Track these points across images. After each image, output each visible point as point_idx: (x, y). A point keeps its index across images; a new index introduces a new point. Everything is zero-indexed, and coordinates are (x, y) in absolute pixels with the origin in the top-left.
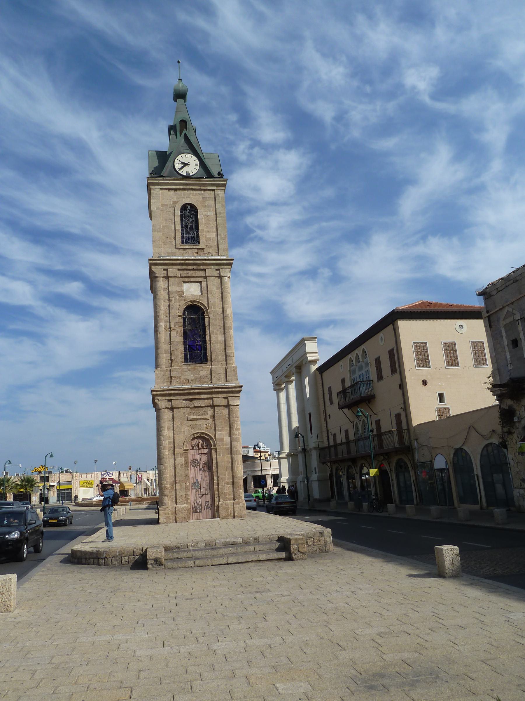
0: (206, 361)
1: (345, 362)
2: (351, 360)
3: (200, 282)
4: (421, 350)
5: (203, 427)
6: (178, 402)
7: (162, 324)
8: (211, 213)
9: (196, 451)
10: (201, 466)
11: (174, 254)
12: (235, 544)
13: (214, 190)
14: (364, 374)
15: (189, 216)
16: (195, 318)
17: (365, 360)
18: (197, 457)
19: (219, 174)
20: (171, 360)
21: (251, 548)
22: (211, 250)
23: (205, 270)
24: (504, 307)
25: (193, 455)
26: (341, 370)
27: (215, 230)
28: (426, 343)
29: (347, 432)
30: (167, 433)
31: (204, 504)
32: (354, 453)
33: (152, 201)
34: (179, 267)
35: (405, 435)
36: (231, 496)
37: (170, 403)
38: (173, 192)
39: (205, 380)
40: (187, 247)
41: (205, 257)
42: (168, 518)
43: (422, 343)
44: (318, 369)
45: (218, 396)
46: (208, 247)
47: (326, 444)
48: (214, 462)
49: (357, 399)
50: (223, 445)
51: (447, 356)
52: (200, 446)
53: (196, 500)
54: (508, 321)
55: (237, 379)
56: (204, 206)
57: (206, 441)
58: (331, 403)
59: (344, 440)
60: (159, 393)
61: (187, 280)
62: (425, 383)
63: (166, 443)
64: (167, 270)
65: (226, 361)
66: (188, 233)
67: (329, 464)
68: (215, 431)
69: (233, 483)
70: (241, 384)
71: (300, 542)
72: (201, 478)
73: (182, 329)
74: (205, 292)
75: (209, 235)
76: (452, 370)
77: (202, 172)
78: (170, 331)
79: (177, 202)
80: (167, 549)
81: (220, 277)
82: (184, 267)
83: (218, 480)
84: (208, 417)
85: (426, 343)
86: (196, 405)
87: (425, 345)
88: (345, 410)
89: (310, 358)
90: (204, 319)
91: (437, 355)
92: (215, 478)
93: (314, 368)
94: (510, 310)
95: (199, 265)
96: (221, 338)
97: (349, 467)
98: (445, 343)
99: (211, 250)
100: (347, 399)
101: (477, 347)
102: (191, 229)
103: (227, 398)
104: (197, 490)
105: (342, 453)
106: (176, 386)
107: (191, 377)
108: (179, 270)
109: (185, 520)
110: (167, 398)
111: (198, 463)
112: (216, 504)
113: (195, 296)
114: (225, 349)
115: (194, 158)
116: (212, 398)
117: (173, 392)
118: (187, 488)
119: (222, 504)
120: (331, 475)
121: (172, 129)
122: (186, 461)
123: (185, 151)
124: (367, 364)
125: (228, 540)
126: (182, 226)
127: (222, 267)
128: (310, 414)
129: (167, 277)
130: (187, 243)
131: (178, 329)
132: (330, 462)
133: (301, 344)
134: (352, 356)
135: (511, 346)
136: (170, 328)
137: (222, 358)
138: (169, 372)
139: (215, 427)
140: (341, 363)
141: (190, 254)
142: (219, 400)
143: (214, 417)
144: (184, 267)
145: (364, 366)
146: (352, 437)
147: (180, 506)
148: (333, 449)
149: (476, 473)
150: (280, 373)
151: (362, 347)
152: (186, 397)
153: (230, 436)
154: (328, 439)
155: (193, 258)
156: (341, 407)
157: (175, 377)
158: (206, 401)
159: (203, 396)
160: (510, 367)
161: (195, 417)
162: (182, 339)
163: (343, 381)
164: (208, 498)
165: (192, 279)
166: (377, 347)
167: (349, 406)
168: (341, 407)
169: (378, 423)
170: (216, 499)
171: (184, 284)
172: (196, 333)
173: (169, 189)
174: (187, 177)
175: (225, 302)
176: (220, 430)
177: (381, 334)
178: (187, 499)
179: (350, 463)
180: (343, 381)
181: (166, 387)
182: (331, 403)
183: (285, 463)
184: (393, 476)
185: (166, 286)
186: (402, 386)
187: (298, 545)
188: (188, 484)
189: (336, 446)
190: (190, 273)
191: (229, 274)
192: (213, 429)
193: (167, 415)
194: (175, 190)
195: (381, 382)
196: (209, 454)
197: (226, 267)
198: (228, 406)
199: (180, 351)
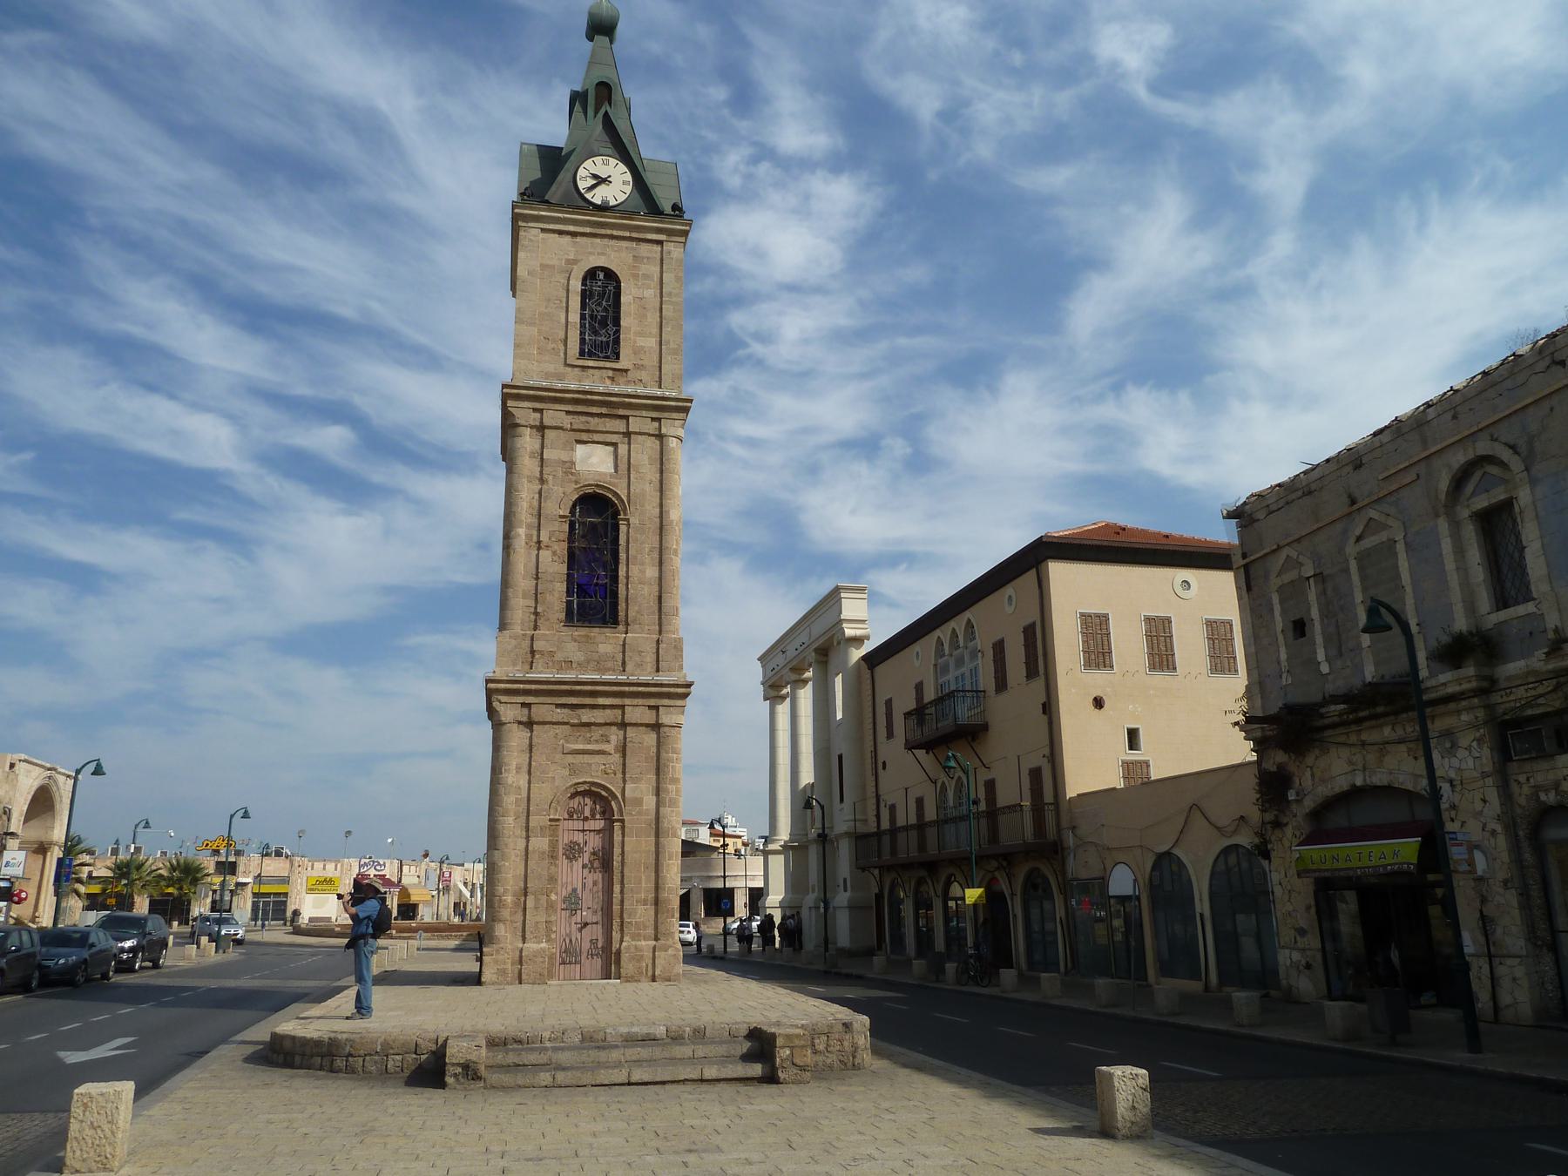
0: (616, 622)
1: (924, 648)
2: (940, 642)
3: (615, 445)
4: (1096, 630)
5: (597, 771)
7: (521, 532)
8: (651, 293)
9: (579, 825)
10: (586, 856)
11: (560, 377)
12: (649, 1040)
13: (660, 243)
14: (968, 674)
15: (601, 297)
16: (597, 523)
17: (971, 644)
18: (579, 838)
19: (675, 207)
20: (536, 614)
21: (685, 1051)
22: (644, 375)
23: (626, 418)
24: (1279, 548)
25: (570, 832)
26: (917, 664)
27: (655, 331)
28: (1106, 616)
29: (920, 802)
30: (514, 778)
31: (586, 945)
32: (932, 849)
33: (521, 255)
34: (570, 408)
35: (1050, 817)
36: (650, 931)
37: (525, 711)
38: (568, 239)
39: (609, 664)
40: (591, 363)
41: (630, 390)
42: (503, 972)
43: (1098, 616)
44: (865, 658)
45: (636, 701)
46: (638, 367)
47: (872, 827)
48: (617, 851)
49: (947, 731)
50: (640, 813)
51: (1151, 646)
52: (587, 813)
53: (569, 935)
54: (1288, 577)
55: (681, 667)
56: (636, 276)
57: (600, 802)
58: (890, 735)
59: (913, 820)
60: (502, 686)
61: (584, 437)
62: (1098, 703)
63: (510, 801)
64: (541, 411)
65: (660, 625)
66: (595, 333)
67: (876, 872)
68: (624, 781)
69: (657, 902)
70: (689, 679)
71: (797, 1042)
72: (584, 885)
73: (565, 545)
74: (625, 467)
75: (641, 342)
76: (1160, 679)
77: (638, 200)
78: (539, 549)
79: (575, 262)
80: (494, 1043)
81: (660, 436)
82: (580, 408)
83: (622, 892)
84: (609, 748)
85: (1106, 616)
86: (585, 719)
87: (1103, 619)
88: (920, 753)
89: (849, 631)
90: (616, 528)
91: (1128, 643)
92: (617, 888)
93: (856, 654)
94: (1294, 554)
95: (614, 407)
96: (651, 572)
97: (920, 882)
98: (1148, 620)
99: (644, 375)
100: (926, 729)
101: (1217, 632)
102: (603, 324)
103: (656, 708)
104: (573, 912)
105: (908, 848)
108: (568, 412)
109: (541, 980)
110: (520, 699)
111: (581, 851)
112: (615, 946)
113: (600, 474)
114: (660, 598)
115: (622, 167)
116: (622, 707)
117: (533, 687)
118: (551, 906)
119: (628, 948)
120: (879, 897)
121: (577, 99)
122: (553, 845)
123: (602, 150)
124: (974, 654)
125: (635, 1029)
126: (583, 317)
127: (666, 415)
128: (840, 757)
129: (541, 428)
130: (591, 355)
131: (556, 547)
132: (880, 868)
134: (943, 633)
135: (1290, 634)
136: (539, 542)
137: (650, 619)
138: (528, 642)
139: (624, 773)
140: (917, 647)
141: (596, 381)
142: (637, 712)
143: (623, 750)
144: (580, 408)
145: (966, 658)
146: (931, 814)
147: (531, 946)
148: (886, 839)
149: (1198, 910)
150: (780, 660)
151: (967, 615)
152: (563, 700)
153: (658, 795)
154: (878, 816)
155: (601, 389)
156: (910, 746)
157: (541, 652)
158: (608, 711)
159: (601, 701)
160: (1286, 680)
161: (581, 747)
162: (564, 568)
163: (919, 687)
164: (596, 932)
165: (596, 437)
166: (999, 618)
167: (929, 746)
168: (910, 746)
169: (990, 785)
170: (616, 935)
171: (578, 446)
172: (596, 559)
173: (561, 233)
174: (603, 208)
175: (667, 493)
176: (636, 780)
177: (1009, 590)
178: (549, 931)
179: (923, 873)
180: (919, 687)
181: (519, 675)
182: (890, 735)
183: (778, 864)
184: (1016, 908)
185: (537, 446)
186: (1049, 708)
187: (792, 1048)
188: (553, 897)
189: (894, 831)
190: (594, 423)
191: (681, 432)
192: (620, 775)
193: (516, 738)
194: (574, 234)
195: (1004, 697)
196: (607, 833)
197: (675, 415)
198: (656, 727)
199: (556, 595)
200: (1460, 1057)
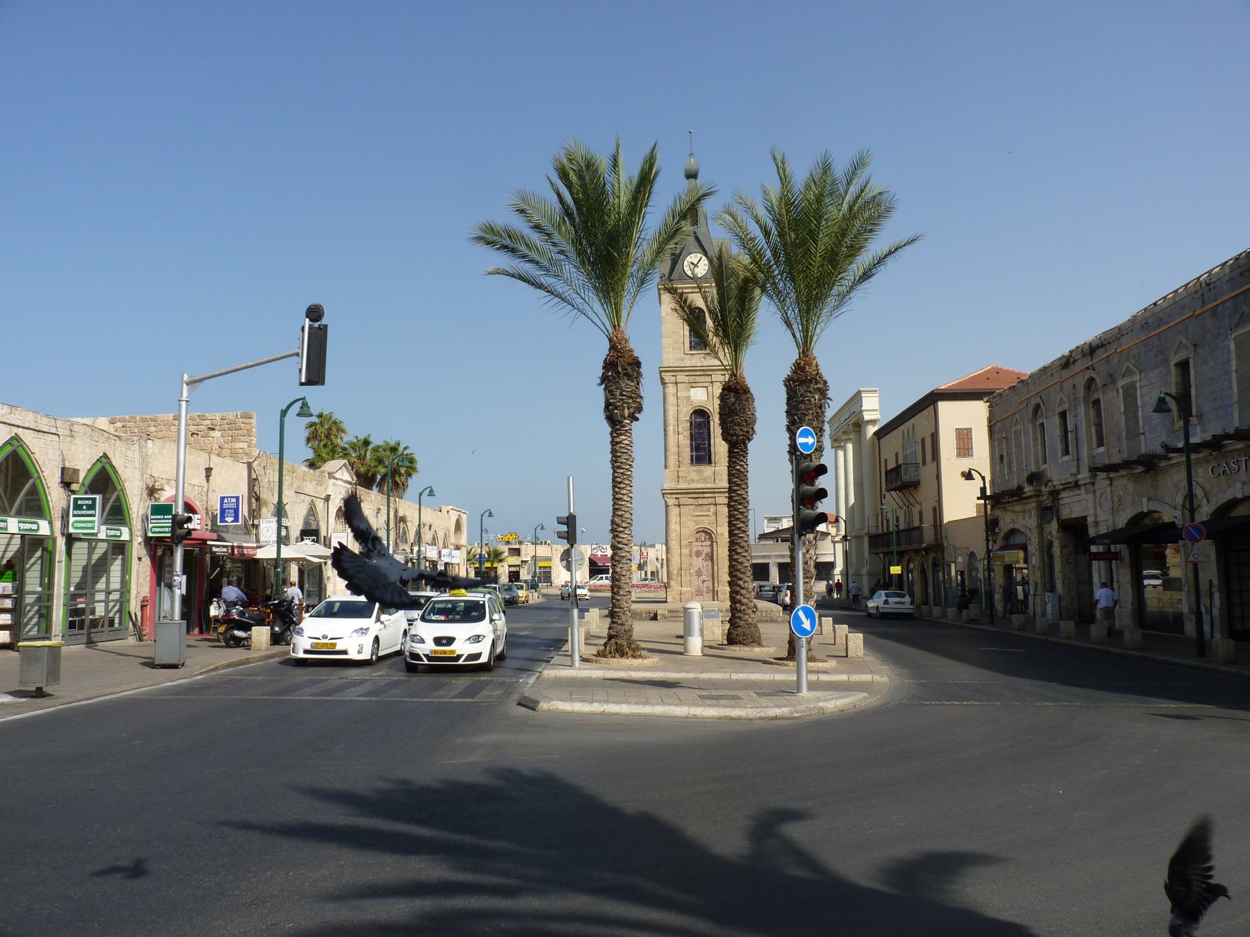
0: (710, 462)
1: (897, 433)
5: (706, 523)
6: (684, 500)
7: (671, 428)
11: (682, 360)
25: (697, 546)
30: (674, 526)
44: (875, 434)
87: (969, 431)
88: (893, 493)
89: (867, 417)
93: (871, 430)
106: (683, 485)
107: (697, 478)
118: (691, 574)
133: (857, 397)
140: (895, 433)
143: (716, 514)
147: (684, 589)
151: (912, 420)
164: (710, 584)
193: (674, 511)
199: (687, 453)
200: (987, 627)
